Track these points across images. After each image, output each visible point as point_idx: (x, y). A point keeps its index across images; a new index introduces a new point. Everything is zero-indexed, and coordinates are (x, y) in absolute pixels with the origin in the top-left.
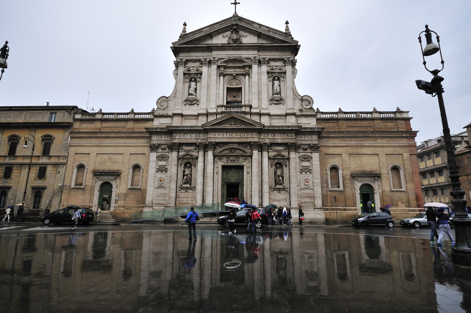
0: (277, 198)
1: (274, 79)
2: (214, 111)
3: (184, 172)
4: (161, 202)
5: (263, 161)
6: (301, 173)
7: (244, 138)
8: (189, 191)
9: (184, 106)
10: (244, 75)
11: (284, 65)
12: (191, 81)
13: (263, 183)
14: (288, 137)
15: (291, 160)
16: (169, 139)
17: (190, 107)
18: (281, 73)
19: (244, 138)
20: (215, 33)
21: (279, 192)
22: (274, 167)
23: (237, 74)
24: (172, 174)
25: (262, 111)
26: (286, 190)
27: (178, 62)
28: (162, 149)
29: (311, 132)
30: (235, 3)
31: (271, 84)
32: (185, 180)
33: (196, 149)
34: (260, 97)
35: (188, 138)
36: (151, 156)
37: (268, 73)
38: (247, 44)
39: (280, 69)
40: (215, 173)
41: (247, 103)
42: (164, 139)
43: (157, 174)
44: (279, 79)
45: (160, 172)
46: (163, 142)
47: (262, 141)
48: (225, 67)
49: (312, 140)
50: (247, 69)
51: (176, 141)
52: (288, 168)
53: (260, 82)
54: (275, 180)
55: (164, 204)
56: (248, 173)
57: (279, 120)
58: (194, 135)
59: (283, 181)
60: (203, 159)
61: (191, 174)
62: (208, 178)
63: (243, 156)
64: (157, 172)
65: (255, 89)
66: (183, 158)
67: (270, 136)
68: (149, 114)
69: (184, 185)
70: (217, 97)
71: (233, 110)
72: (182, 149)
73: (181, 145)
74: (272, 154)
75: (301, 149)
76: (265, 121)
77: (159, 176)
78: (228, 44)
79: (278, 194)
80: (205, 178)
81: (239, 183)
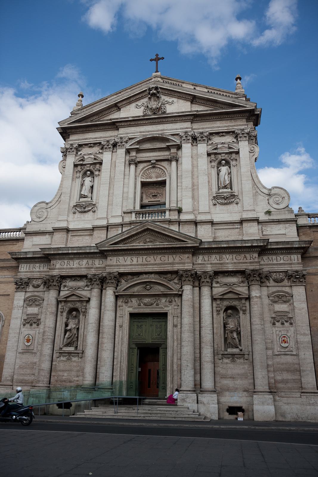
0: (230, 372)
1: (220, 164)
2: (119, 220)
3: (67, 325)
4: (26, 378)
5: (203, 305)
6: (274, 324)
7: (166, 264)
8: (74, 359)
9: (71, 215)
10: (169, 161)
11: (235, 140)
12: (85, 175)
13: (203, 345)
14: (245, 261)
15: (254, 301)
16: (45, 269)
17: (82, 215)
18: (231, 153)
19: (166, 264)
20: (125, 102)
21: (233, 361)
22: (222, 315)
23: (157, 161)
24: (47, 329)
25: (200, 218)
26: (246, 356)
27: (67, 149)
28: (33, 286)
29: (287, 249)
31: (214, 172)
32: (68, 338)
33: (87, 286)
34: (196, 194)
35: (75, 266)
36: (15, 298)
37: (209, 155)
38: (173, 113)
39: (230, 148)
40: (117, 328)
41: (174, 205)
42: (37, 270)
43: (23, 330)
44: (228, 163)
45: (28, 326)
46: (37, 275)
47: (199, 269)
48: (138, 151)
49: (291, 264)
50: (173, 150)
51: (55, 273)
52: (248, 315)
53: (195, 170)
54: (226, 339)
55: (32, 383)
56: (175, 326)
57: (230, 231)
58: (85, 261)
59: (240, 341)
60: (99, 302)
61: (78, 329)
62: (105, 336)
63: (165, 295)
64: (24, 325)
65: (187, 182)
66: (66, 301)
67: (214, 258)
68: (19, 230)
70: (124, 198)
71: (149, 218)
72: (65, 286)
73: (63, 278)
74: (218, 290)
75: (271, 281)
77: (26, 333)
78: (143, 116)
79: (231, 366)
80: (100, 335)
81: (161, 345)
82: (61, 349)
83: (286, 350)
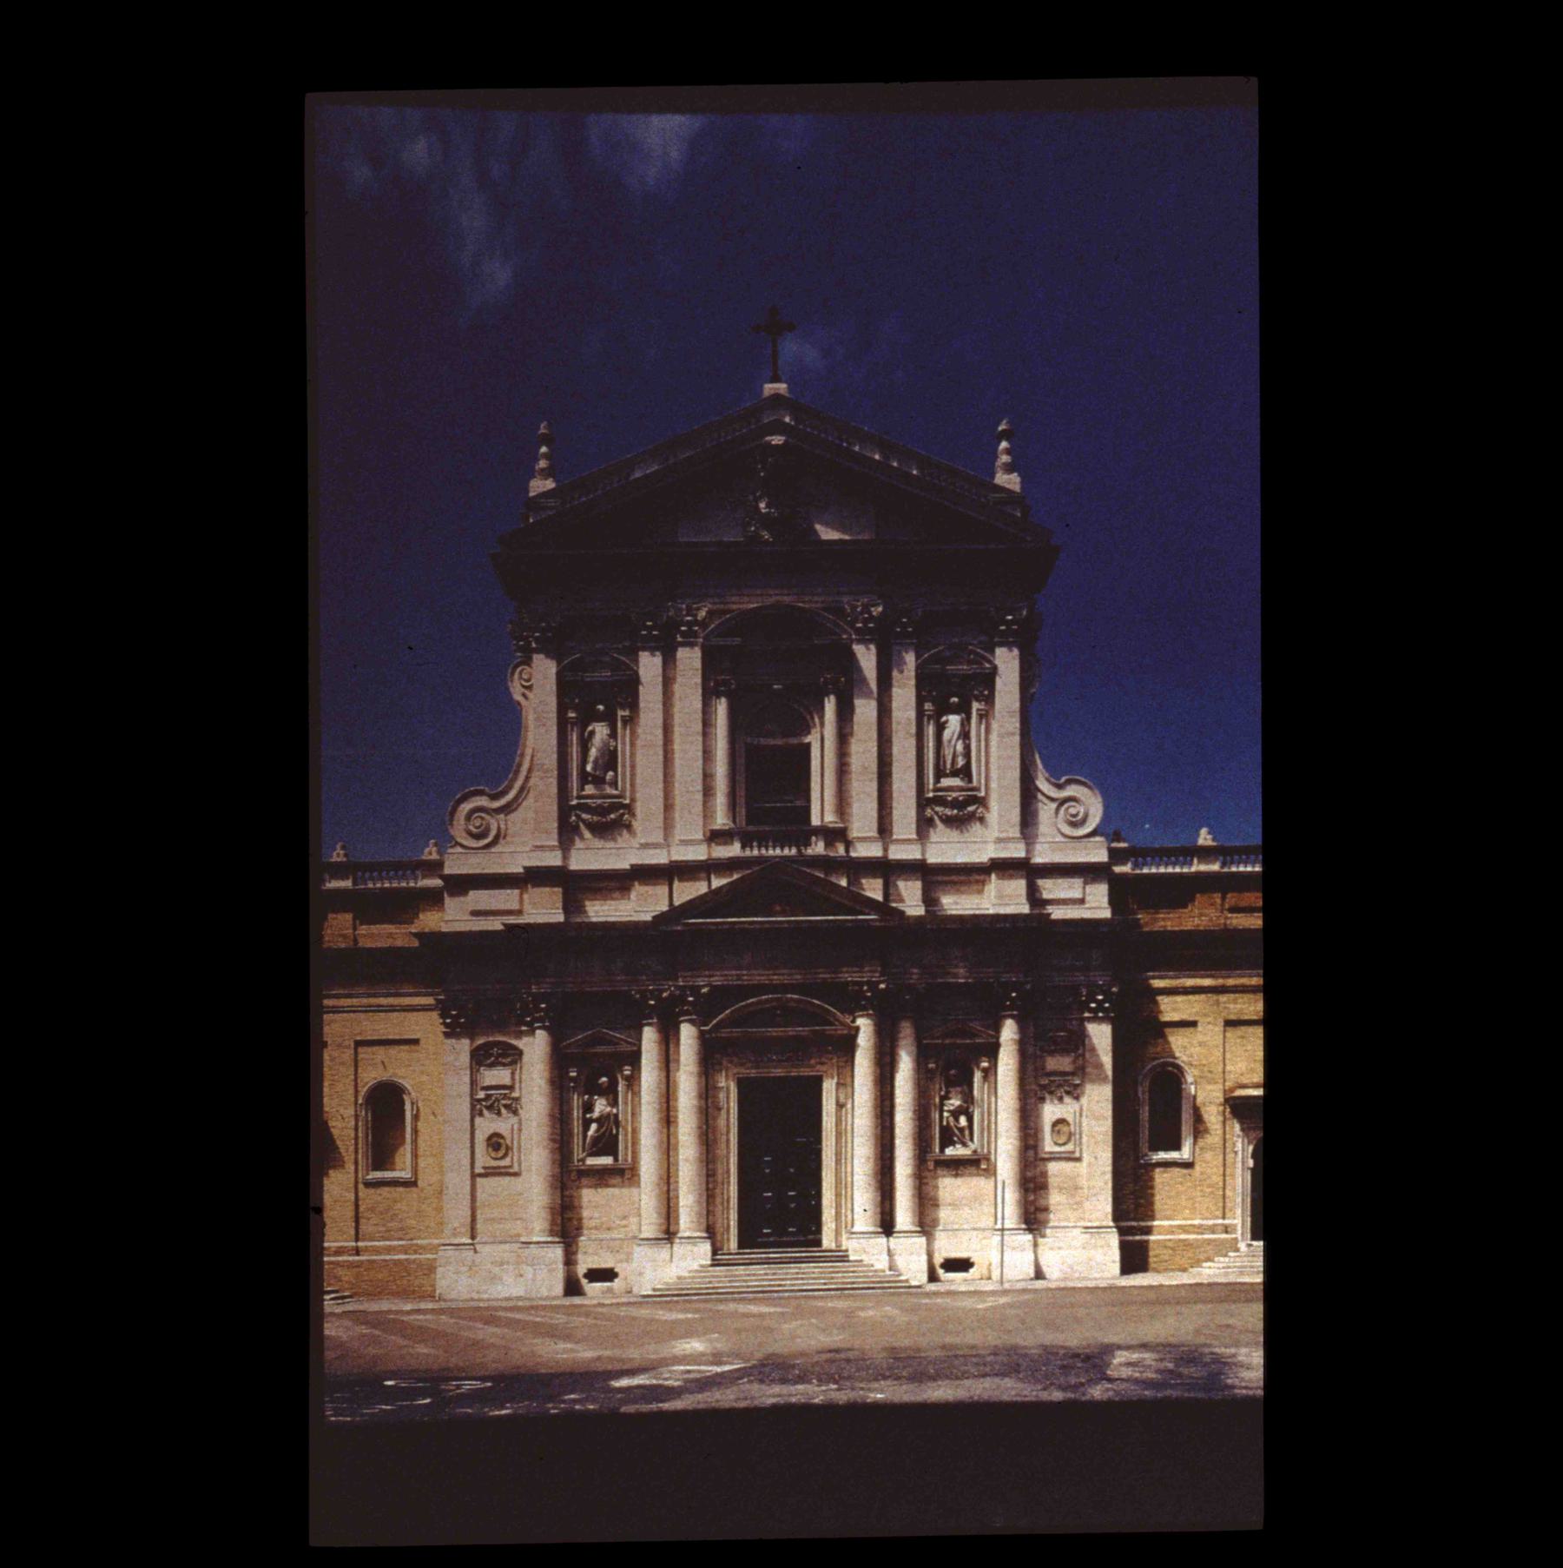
3: (588, 1107)
32: (596, 1140)
43: (478, 1120)
44: (963, 709)
56: (840, 1106)
61: (616, 1116)
69: (591, 1161)
82: (583, 1160)
83: (1062, 1149)
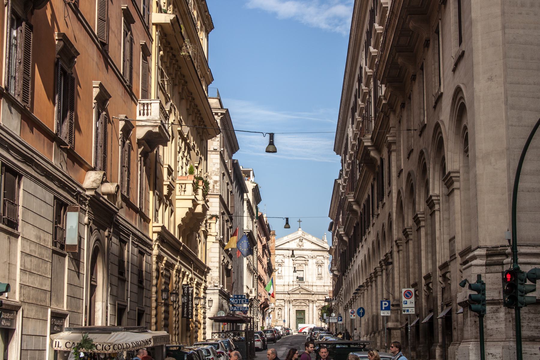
25: (314, 284)
30: (300, 221)
74: (317, 304)
76: (315, 289)
